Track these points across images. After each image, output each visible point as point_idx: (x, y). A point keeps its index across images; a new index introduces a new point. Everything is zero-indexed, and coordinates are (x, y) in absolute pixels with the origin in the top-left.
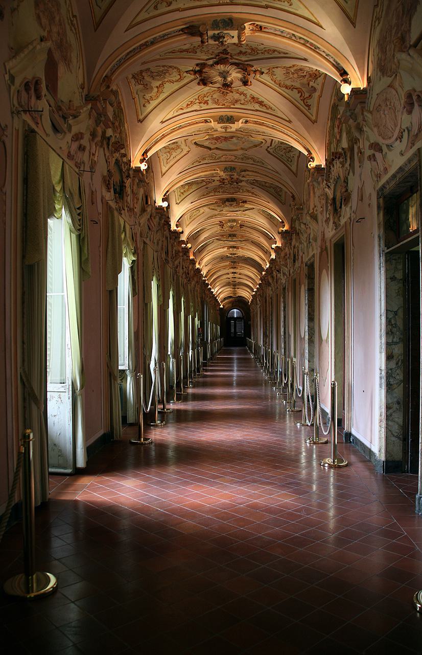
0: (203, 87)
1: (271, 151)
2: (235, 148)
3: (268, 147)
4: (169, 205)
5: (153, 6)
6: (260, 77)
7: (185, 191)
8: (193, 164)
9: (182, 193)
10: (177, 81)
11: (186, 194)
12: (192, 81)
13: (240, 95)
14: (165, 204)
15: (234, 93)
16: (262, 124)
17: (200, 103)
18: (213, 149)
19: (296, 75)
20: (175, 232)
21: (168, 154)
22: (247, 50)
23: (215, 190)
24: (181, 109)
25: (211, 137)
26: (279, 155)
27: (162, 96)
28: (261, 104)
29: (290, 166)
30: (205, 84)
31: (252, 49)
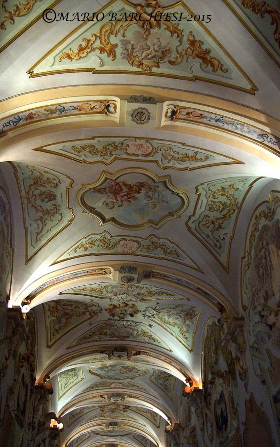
1: (192, 226)
7: (60, 328)
8: (75, 250)
17: (102, 50)
21: (39, 222)
24: (69, 56)
28: (204, 60)
29: (217, 255)
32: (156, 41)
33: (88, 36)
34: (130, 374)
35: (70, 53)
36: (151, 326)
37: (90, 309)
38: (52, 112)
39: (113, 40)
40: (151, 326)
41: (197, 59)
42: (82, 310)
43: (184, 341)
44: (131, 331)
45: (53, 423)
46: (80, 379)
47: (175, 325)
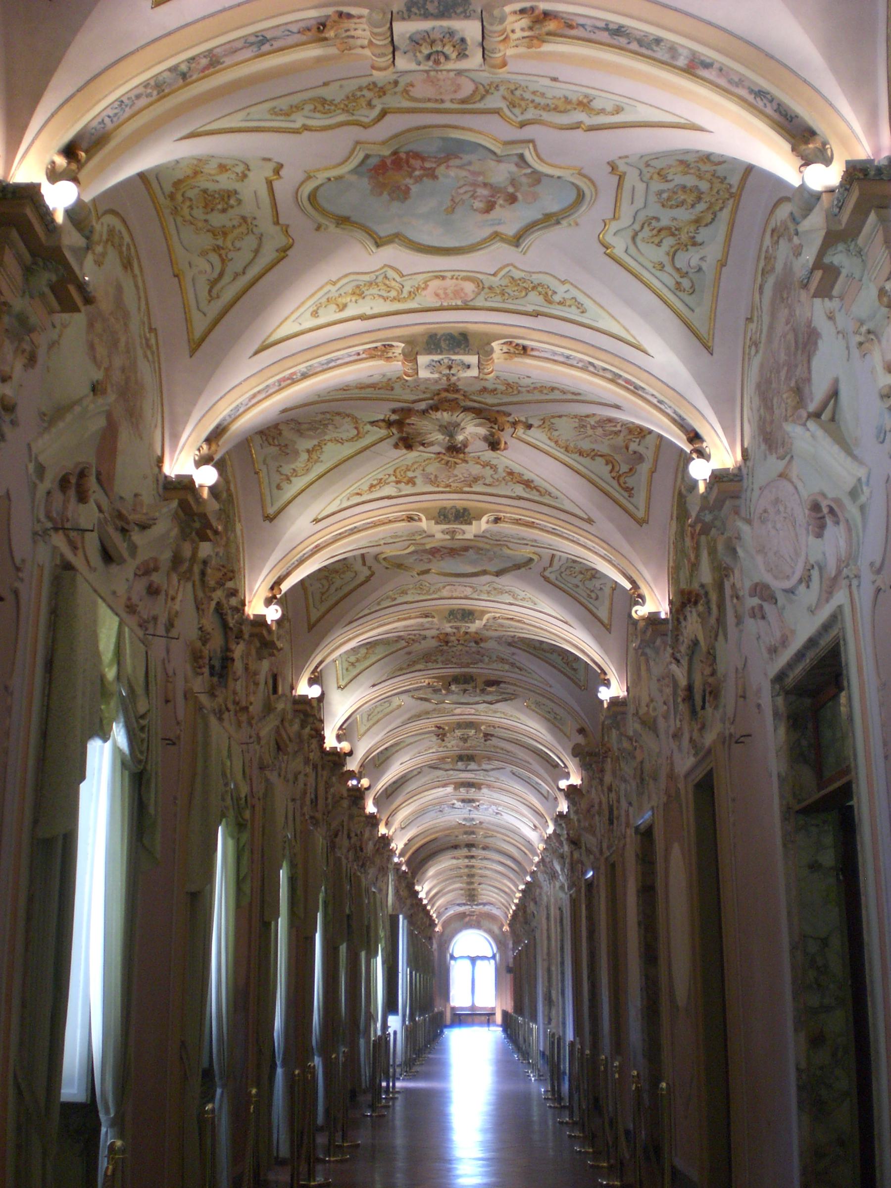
0: (404, 451)
1: (552, 577)
3: (545, 569)
4: (323, 694)
5: (311, 309)
7: (358, 660)
9: (353, 664)
10: (351, 440)
11: (360, 667)
12: (382, 440)
13: (484, 466)
15: (471, 463)
16: (531, 525)
19: (600, 429)
20: (334, 752)
21: (325, 582)
22: (497, 386)
23: (428, 657)
24: (358, 494)
25: (421, 548)
26: (570, 585)
30: (409, 447)
31: (508, 384)
35: (359, 491)
38: (340, 534)
43: (571, 673)
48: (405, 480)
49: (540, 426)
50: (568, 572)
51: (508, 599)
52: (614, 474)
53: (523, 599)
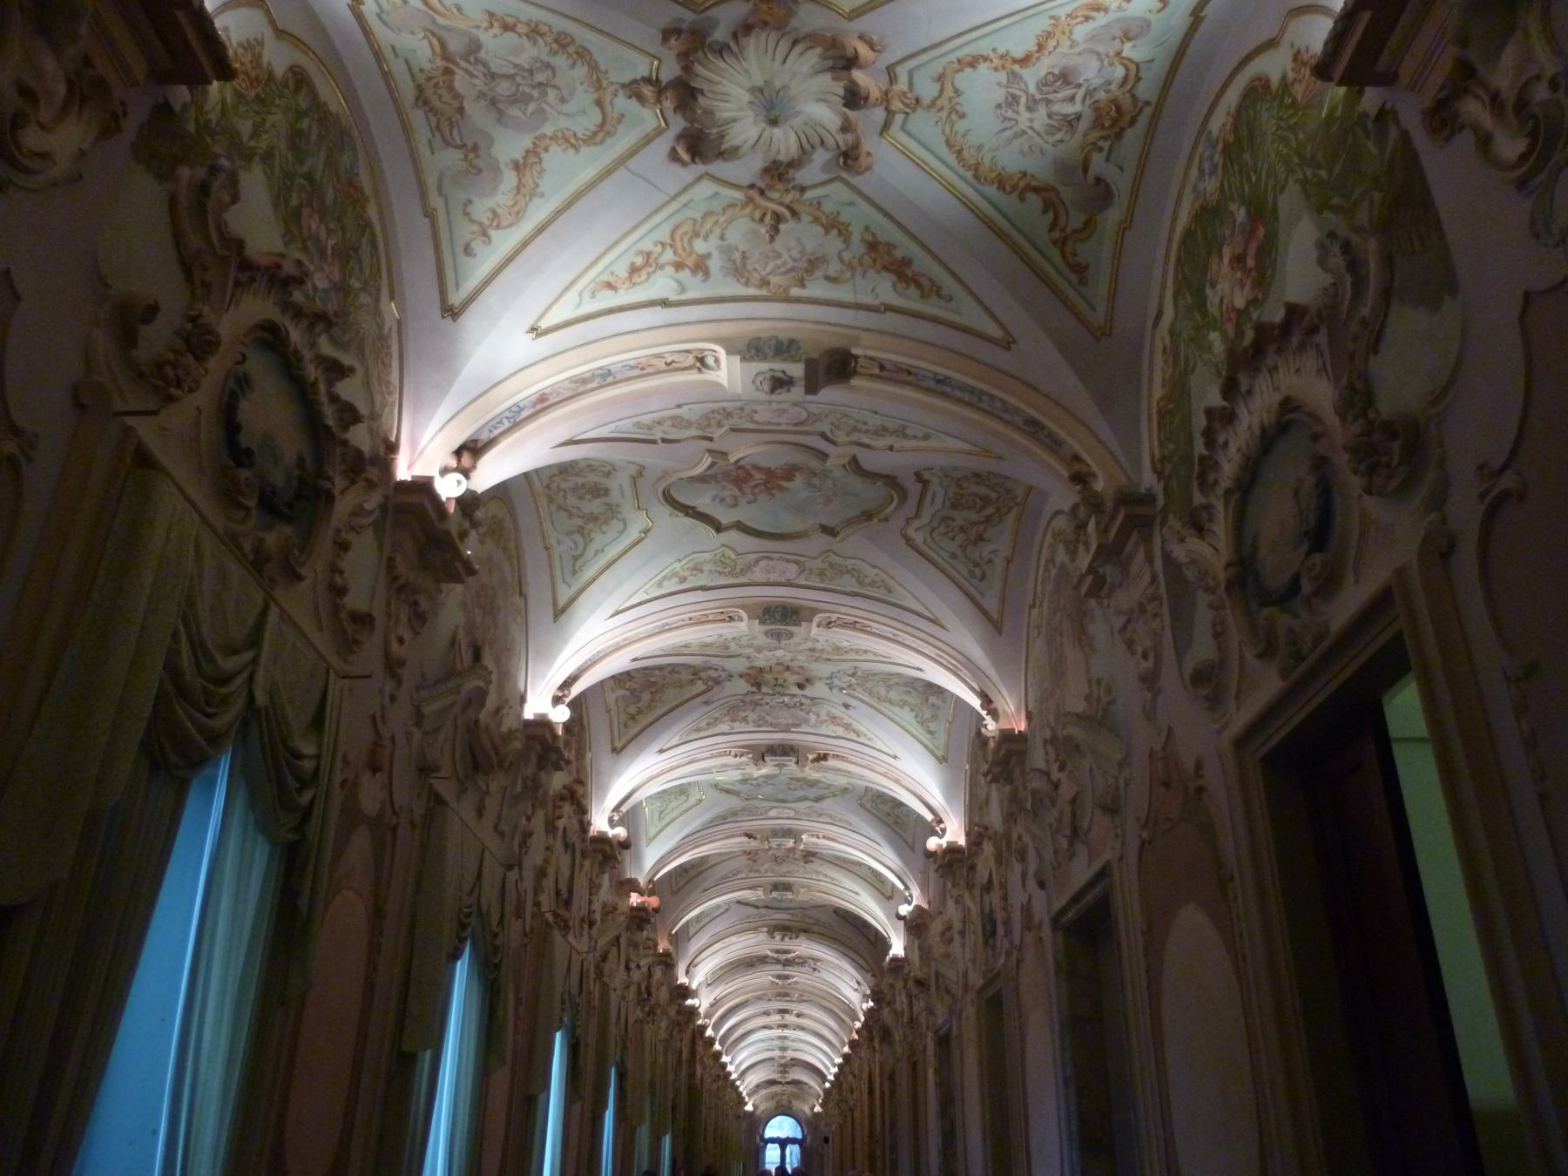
1: (919, 538)
2: (799, 527)
3: (908, 521)
6: (903, 128)
8: (660, 585)
9: (633, 717)
10: (591, 139)
12: (647, 140)
14: (560, 715)
15: (806, 219)
17: (679, 266)
18: (727, 528)
20: (602, 839)
21: (578, 537)
27: (538, 212)
32: (792, 243)
33: (647, 245)
34: (812, 793)
35: (611, 279)
36: (847, 706)
37: (703, 674)
38: (584, 381)
39: (700, 246)
40: (847, 706)
41: (885, 274)
42: (685, 676)
43: (925, 738)
44: (802, 714)
45: (635, 899)
46: (693, 800)
47: (903, 704)
48: (690, 262)
49: (933, 103)
50: (942, 529)
51: (848, 583)
52: (1056, 234)
53: (872, 584)
